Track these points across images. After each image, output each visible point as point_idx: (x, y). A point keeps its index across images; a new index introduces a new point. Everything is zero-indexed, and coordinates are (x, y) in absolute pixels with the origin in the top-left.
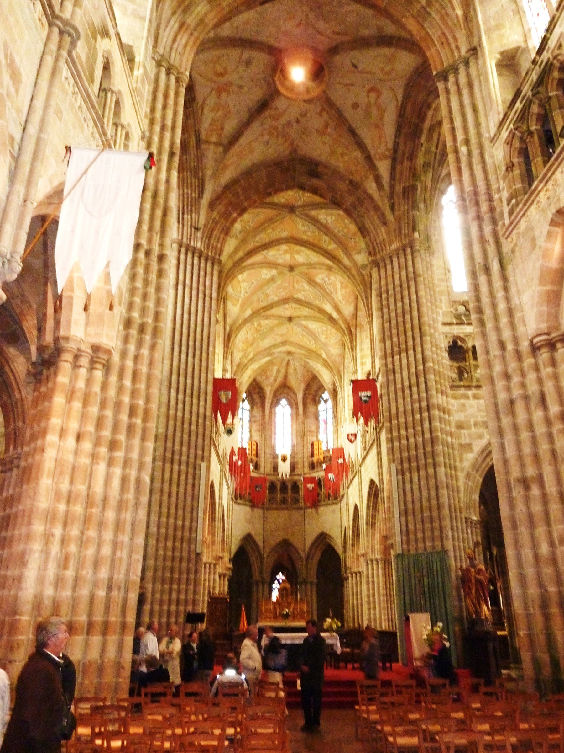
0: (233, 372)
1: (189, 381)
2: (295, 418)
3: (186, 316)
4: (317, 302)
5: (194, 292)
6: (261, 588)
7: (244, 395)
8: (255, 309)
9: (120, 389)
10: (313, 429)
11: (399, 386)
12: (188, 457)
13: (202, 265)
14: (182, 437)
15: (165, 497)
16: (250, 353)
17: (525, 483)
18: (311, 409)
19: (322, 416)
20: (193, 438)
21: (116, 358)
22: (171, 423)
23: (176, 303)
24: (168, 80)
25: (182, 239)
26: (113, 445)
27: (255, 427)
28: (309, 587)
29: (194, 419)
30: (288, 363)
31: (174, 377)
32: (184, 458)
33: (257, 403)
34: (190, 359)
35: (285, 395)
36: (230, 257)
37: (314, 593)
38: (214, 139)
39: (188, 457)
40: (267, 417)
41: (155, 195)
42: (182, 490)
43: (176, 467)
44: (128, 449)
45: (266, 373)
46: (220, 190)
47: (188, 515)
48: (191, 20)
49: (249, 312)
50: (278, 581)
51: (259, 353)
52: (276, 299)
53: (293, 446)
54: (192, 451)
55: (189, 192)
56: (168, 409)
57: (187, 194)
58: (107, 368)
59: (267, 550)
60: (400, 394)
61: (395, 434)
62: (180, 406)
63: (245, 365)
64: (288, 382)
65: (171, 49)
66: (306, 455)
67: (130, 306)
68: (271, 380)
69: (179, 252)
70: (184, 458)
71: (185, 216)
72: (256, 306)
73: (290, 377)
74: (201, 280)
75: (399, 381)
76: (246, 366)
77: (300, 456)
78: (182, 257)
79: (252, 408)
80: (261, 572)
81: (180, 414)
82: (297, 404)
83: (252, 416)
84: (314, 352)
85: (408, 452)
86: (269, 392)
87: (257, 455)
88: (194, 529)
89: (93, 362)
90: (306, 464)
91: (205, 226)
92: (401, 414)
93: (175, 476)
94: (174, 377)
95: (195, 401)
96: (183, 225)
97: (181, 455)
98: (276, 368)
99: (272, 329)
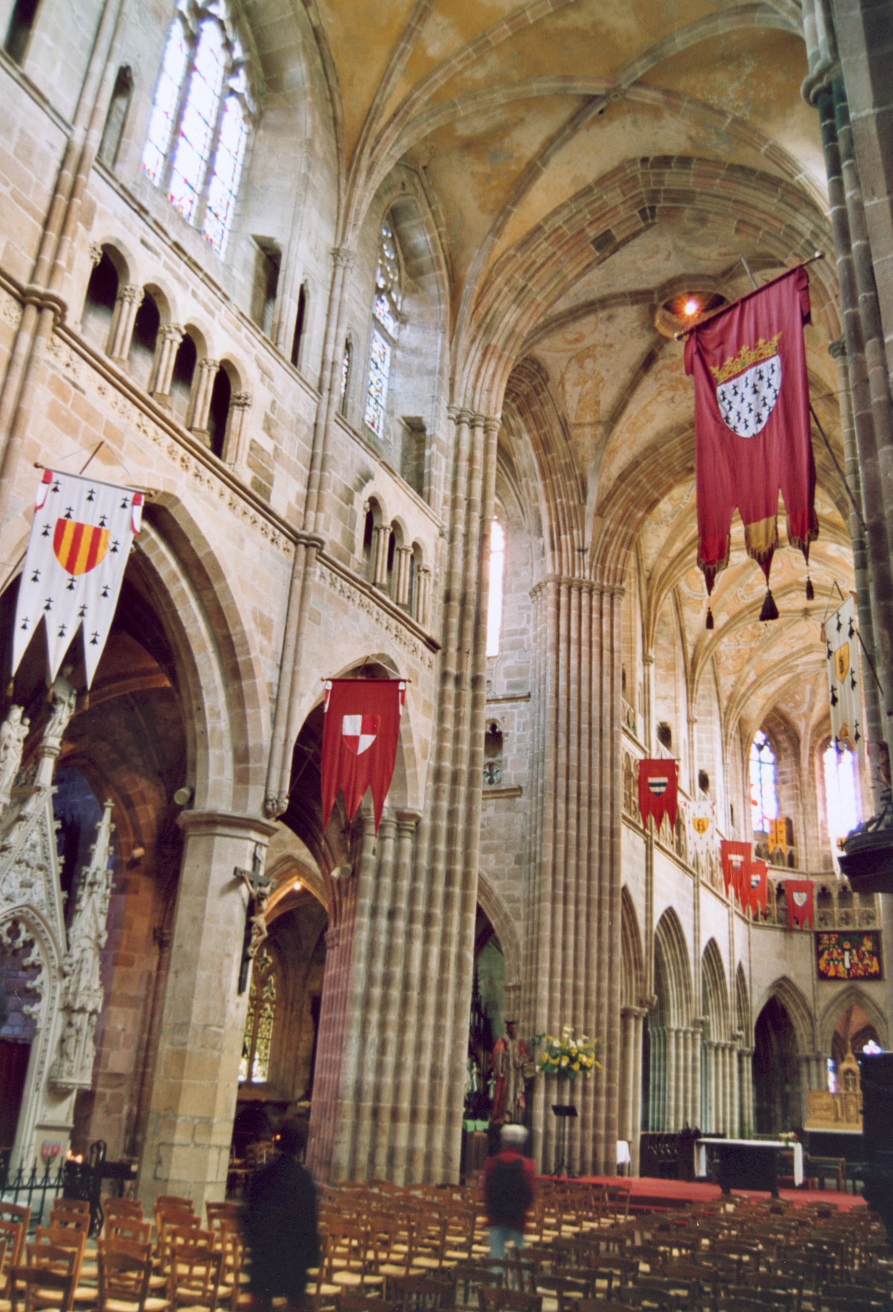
0: (723, 710)
1: (584, 783)
3: (574, 687)
5: (585, 648)
8: (733, 612)
9: (434, 855)
12: (589, 892)
13: (595, 603)
16: (748, 674)
20: (596, 865)
21: (427, 822)
23: (557, 670)
24: (473, 435)
25: (561, 573)
26: (429, 920)
27: (786, 792)
29: (596, 836)
32: (583, 894)
33: (785, 750)
36: (662, 554)
38: (588, 419)
40: (805, 773)
41: (464, 602)
43: (571, 908)
45: (793, 697)
48: (497, 340)
51: (764, 673)
54: (595, 883)
55: (564, 500)
57: (561, 503)
58: (416, 833)
59: (822, 1004)
62: (573, 821)
63: (744, 695)
65: (474, 388)
67: (440, 753)
68: (805, 708)
69: (558, 593)
71: (563, 537)
78: (563, 599)
79: (778, 760)
80: (813, 1042)
81: (573, 833)
86: (804, 729)
87: (791, 841)
89: (399, 829)
91: (593, 545)
93: (571, 921)
94: (562, 781)
96: (560, 550)
97: (577, 889)
98: (808, 688)
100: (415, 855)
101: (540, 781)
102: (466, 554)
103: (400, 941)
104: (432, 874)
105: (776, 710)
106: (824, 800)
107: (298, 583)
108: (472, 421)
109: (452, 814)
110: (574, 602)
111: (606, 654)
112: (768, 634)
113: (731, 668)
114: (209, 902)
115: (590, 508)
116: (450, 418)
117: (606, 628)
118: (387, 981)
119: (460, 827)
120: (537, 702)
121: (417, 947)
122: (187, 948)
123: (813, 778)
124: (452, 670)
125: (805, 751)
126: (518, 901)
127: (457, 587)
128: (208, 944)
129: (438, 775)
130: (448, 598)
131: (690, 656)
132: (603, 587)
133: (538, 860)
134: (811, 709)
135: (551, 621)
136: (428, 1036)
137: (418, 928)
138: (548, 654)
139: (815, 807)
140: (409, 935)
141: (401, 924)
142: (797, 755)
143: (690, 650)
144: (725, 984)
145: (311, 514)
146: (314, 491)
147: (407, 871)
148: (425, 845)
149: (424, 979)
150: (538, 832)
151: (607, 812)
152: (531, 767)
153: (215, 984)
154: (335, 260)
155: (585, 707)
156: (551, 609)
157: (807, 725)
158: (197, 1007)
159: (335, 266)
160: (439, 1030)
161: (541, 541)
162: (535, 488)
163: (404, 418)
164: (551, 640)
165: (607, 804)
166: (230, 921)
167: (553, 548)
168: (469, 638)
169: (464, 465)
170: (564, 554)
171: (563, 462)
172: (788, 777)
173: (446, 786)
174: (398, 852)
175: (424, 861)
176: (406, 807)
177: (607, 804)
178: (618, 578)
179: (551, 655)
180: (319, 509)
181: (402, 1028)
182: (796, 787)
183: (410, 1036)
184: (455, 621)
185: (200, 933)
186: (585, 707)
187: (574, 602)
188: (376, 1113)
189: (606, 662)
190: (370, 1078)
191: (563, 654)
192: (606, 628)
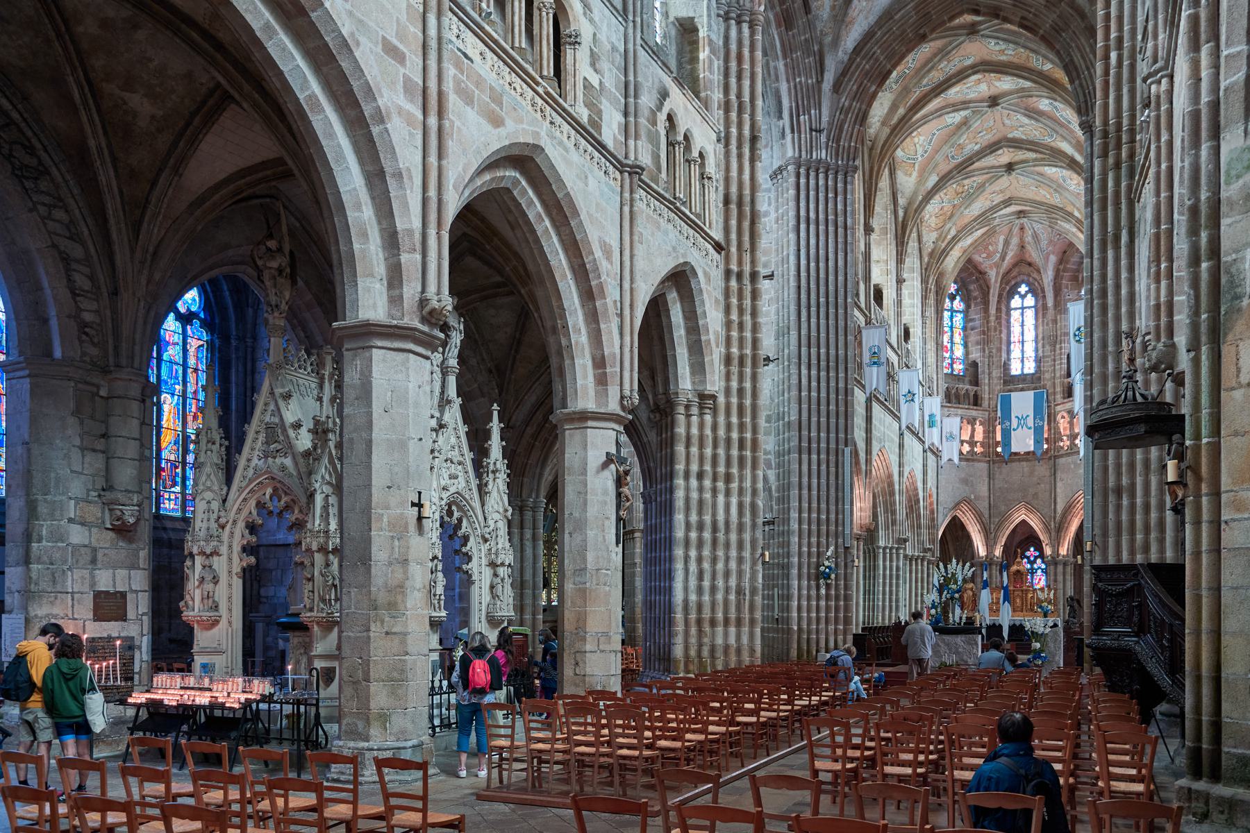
0: (924, 267)
5: (822, 228)
7: (953, 288)
9: (729, 427)
12: (828, 443)
14: (819, 422)
15: (805, 492)
20: (833, 420)
21: (721, 399)
22: (805, 406)
23: (799, 250)
25: (800, 157)
26: (728, 478)
27: (973, 338)
29: (833, 396)
30: (1022, 229)
31: (804, 350)
32: (823, 445)
33: (976, 298)
34: (823, 322)
35: (1025, 278)
39: (828, 443)
40: (992, 318)
42: (823, 481)
43: (814, 457)
45: (986, 248)
47: (833, 508)
49: (933, 179)
54: (833, 435)
56: (800, 391)
58: (715, 411)
62: (814, 384)
63: (944, 250)
64: (1027, 256)
69: (798, 176)
70: (823, 445)
73: (1028, 247)
74: (830, 205)
76: (945, 253)
79: (968, 307)
81: (814, 394)
83: (967, 319)
86: (993, 276)
87: (975, 382)
89: (701, 408)
93: (814, 467)
94: (804, 350)
95: (832, 374)
98: (1002, 238)
99: (982, 187)
100: (715, 428)
101: (786, 351)
103: (708, 496)
104: (728, 441)
105: (969, 261)
106: (1009, 343)
109: (741, 391)
110: (812, 182)
111: (840, 230)
113: (933, 225)
114: (589, 478)
115: (827, 85)
116: (719, 15)
117: (840, 207)
118: (701, 527)
119: (748, 402)
120: (781, 280)
121: (721, 499)
122: (576, 515)
123: (1000, 323)
126: (769, 453)
128: (592, 511)
129: (728, 360)
131: (900, 219)
133: (786, 419)
134: (1003, 258)
135: (792, 204)
137: (721, 485)
138: (790, 235)
139: (1000, 350)
140: (714, 491)
141: (707, 483)
142: (986, 303)
143: (901, 213)
144: (919, 508)
145: (631, 142)
146: (632, 119)
148: (721, 419)
149: (727, 523)
150: (786, 395)
151: (842, 375)
152: (777, 339)
153: (600, 539)
155: (822, 282)
156: (792, 192)
157: (998, 273)
161: (781, 123)
162: (776, 68)
163: (677, 19)
164: (792, 223)
165: (841, 368)
166: (605, 492)
167: (793, 131)
170: (803, 136)
171: (803, 38)
172: (977, 323)
173: (735, 369)
174: (701, 426)
175: (721, 432)
176: (706, 389)
177: (841, 368)
179: (792, 236)
182: (984, 332)
185: (585, 503)
186: (822, 282)
187: (812, 182)
191: (803, 234)
192: (840, 207)
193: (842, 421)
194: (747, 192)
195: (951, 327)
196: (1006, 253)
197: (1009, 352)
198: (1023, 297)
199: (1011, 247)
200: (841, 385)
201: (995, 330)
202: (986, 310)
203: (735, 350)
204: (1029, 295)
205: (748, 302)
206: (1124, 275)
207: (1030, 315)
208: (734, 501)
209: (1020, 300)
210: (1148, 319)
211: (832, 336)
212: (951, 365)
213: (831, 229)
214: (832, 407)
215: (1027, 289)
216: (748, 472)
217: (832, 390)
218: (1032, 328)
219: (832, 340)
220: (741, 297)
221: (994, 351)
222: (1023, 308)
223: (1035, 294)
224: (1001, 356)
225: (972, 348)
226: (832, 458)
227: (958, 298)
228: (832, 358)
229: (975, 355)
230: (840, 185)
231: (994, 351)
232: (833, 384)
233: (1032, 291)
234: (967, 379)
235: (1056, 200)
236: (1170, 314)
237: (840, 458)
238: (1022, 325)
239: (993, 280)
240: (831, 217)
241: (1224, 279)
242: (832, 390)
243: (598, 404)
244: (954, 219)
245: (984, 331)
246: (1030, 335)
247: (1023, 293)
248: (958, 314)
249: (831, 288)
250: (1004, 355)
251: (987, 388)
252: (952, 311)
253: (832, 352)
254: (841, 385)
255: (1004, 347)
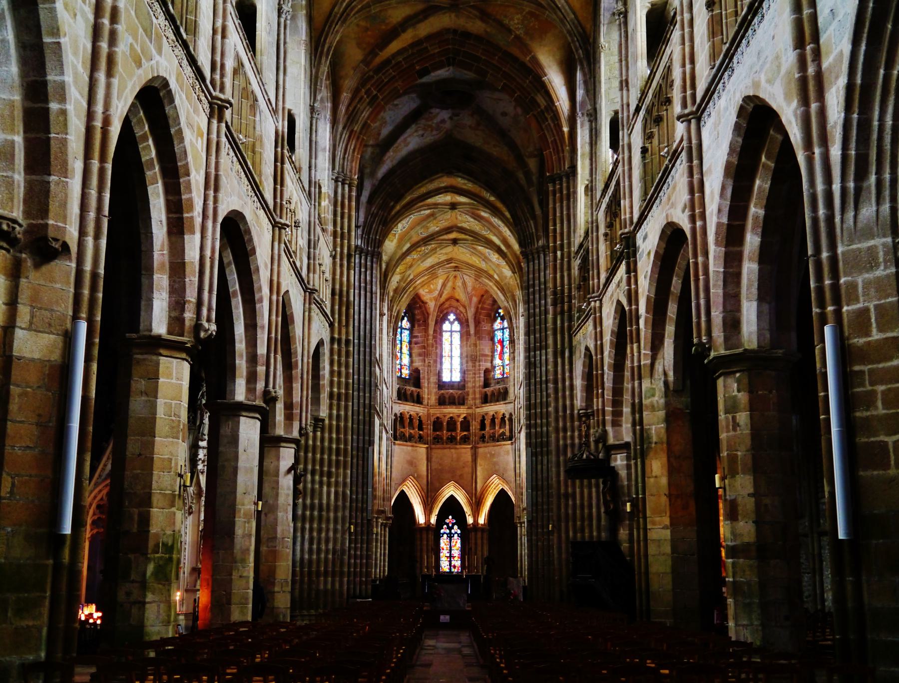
2: (465, 338)
4: (484, 233)
6: (424, 536)
10: (487, 351)
11: (538, 379)
17: (566, 495)
18: (485, 327)
19: (498, 335)
20: (361, 427)
21: (327, 422)
24: (343, 189)
26: (329, 475)
27: (416, 351)
28: (479, 535)
29: (361, 409)
30: (455, 277)
33: (419, 321)
37: (485, 541)
38: (371, 142)
40: (431, 337)
44: (337, 476)
46: (377, 183)
47: (360, 490)
49: (408, 245)
50: (448, 524)
52: (437, 229)
53: (464, 372)
54: (361, 438)
60: (538, 386)
61: (533, 422)
63: (404, 289)
66: (477, 385)
72: (415, 239)
73: (457, 289)
74: (362, 277)
75: (538, 375)
77: (470, 385)
82: (467, 321)
83: (411, 336)
84: (486, 272)
85: (542, 438)
88: (365, 500)
90: (478, 396)
92: (539, 406)
102: (341, 266)
103: (317, 486)
104: (330, 449)
106: (441, 357)
107: (307, 314)
108: (344, 180)
109: (338, 416)
111: (368, 294)
112: (427, 251)
114: (281, 479)
117: (368, 278)
121: (325, 488)
124: (336, 336)
125: (432, 323)
127: (337, 287)
130: (333, 293)
131: (383, 270)
132: (368, 250)
136: (331, 534)
137: (325, 479)
140: (321, 483)
143: (384, 266)
147: (318, 450)
148: (326, 435)
151: (367, 395)
153: (285, 518)
154: (312, 113)
155: (356, 329)
158: (279, 529)
159: (312, 118)
160: (335, 531)
166: (288, 489)
168: (344, 318)
169: (339, 209)
173: (335, 402)
175: (326, 444)
178: (377, 245)
180: (314, 272)
181: (320, 531)
182: (424, 347)
183: (323, 535)
184: (337, 307)
185: (277, 495)
186: (356, 329)
188: (310, 572)
189: (368, 301)
190: (306, 556)
192: (368, 278)
193: (367, 427)
194: (345, 289)
195: (401, 341)
196: (443, 292)
197: (441, 363)
198: (452, 323)
199: (447, 288)
200: (367, 402)
201: (433, 347)
202: (426, 330)
203: (335, 390)
204: (456, 323)
205: (343, 359)
206: (567, 374)
207: (457, 337)
208: (333, 490)
209: (449, 325)
210: (581, 401)
211: (361, 367)
212: (400, 370)
213: (362, 292)
214: (361, 417)
215: (454, 317)
216: (341, 471)
217: (361, 406)
218: (458, 347)
219: (362, 370)
220: (339, 356)
221: (432, 362)
222: (451, 331)
223: (461, 323)
224: (436, 367)
225: (415, 358)
226: (360, 454)
227: (406, 318)
228: (362, 382)
229: (418, 364)
230: (369, 263)
231: (432, 362)
232: (362, 401)
233: (458, 319)
234: (412, 381)
235: (483, 265)
236: (604, 415)
237: (366, 454)
238: (451, 344)
239: (432, 309)
240: (363, 285)
241: (645, 435)
242: (361, 406)
243: (286, 432)
244: (413, 269)
245: (424, 346)
246: (457, 352)
247: (452, 320)
248: (406, 331)
249: (362, 333)
250: (439, 366)
251: (426, 390)
252: (402, 328)
253: (362, 378)
254: (367, 402)
255: (439, 360)
